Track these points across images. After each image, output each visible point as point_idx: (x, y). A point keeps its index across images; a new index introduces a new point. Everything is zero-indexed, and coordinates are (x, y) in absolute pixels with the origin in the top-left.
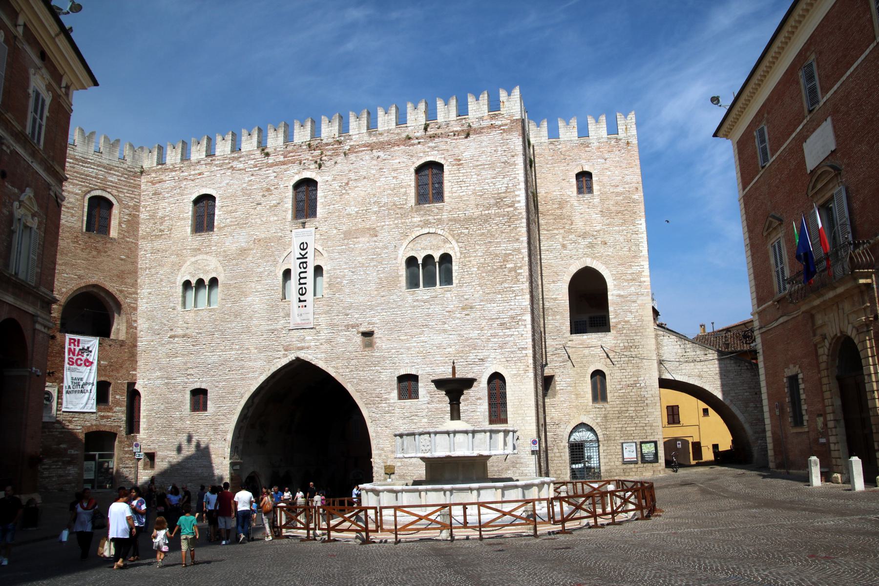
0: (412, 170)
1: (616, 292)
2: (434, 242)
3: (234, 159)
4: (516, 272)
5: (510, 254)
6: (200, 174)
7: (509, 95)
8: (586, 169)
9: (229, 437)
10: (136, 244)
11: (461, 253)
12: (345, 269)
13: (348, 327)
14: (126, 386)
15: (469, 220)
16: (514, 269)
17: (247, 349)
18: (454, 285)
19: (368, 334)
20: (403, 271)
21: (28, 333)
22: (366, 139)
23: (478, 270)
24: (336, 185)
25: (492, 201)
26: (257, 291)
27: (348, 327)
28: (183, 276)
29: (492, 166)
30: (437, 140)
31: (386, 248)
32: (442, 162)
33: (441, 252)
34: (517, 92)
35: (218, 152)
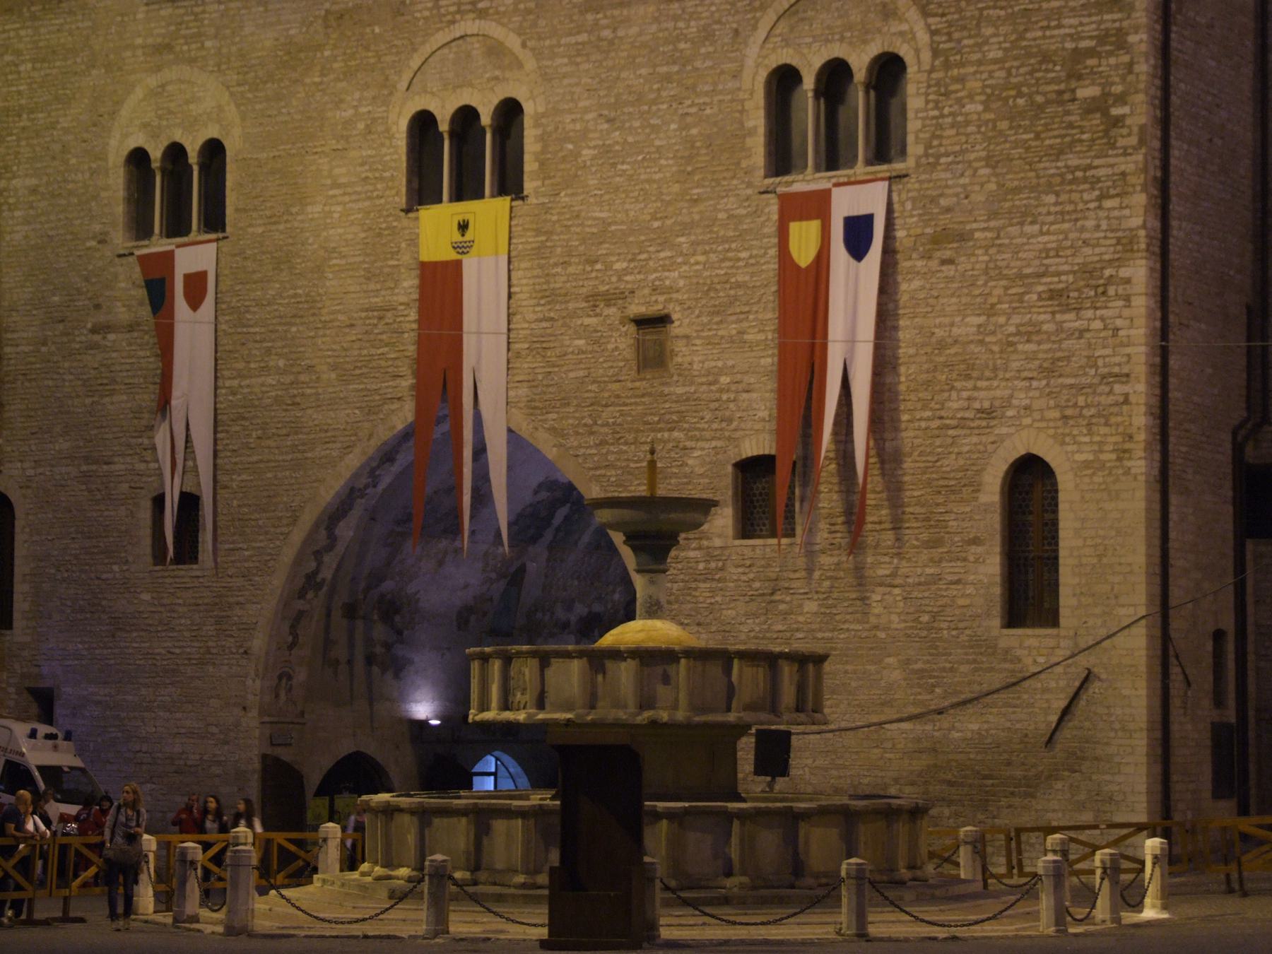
2: (855, 17)
4: (1105, 113)
5: (1091, 52)
9: (258, 643)
11: (936, 53)
12: (586, 110)
13: (595, 300)
16: (1098, 106)
17: (310, 368)
18: (910, 162)
19: (655, 323)
20: (757, 120)
23: (987, 109)
26: (336, 185)
27: (595, 300)
28: (125, 136)
31: (707, 35)
33: (874, 49)
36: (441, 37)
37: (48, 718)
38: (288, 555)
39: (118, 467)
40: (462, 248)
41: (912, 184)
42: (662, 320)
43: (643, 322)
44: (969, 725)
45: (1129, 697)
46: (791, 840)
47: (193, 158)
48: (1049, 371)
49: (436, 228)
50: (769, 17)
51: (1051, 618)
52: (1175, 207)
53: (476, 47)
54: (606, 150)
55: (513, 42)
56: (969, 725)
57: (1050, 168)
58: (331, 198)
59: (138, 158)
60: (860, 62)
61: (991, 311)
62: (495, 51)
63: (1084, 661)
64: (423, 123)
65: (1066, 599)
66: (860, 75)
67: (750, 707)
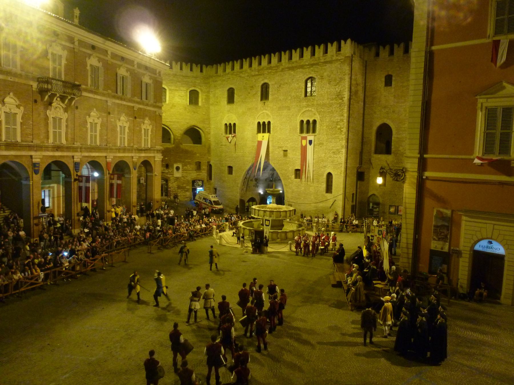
0: (304, 81)
1: (395, 136)
3: (241, 72)
6: (229, 79)
7: (345, 43)
8: (390, 73)
9: (239, 185)
10: (209, 107)
14: (207, 163)
15: (324, 105)
21: (152, 163)
22: (287, 66)
24: (276, 86)
25: (334, 97)
29: (335, 80)
30: (314, 67)
32: (316, 77)
33: (313, 119)
34: (349, 41)
35: (235, 68)
36: (261, 112)
37: (215, 193)
38: (243, 175)
39: (224, 162)
40: (263, 139)
41: (317, 137)
42: (286, 151)
43: (284, 151)
44: (321, 205)
45: (340, 203)
46: (286, 235)
47: (232, 125)
48: (333, 162)
49: (260, 135)
50: (300, 114)
51: (331, 192)
52: (349, 141)
53: (265, 114)
54: (280, 129)
55: (270, 114)
56: (321, 205)
57: (334, 136)
58: (248, 131)
59: (226, 124)
60: (311, 121)
61: (326, 154)
62: (267, 115)
63: (335, 198)
64: (259, 123)
65: (333, 191)
66: (311, 122)
67: (284, 217)
